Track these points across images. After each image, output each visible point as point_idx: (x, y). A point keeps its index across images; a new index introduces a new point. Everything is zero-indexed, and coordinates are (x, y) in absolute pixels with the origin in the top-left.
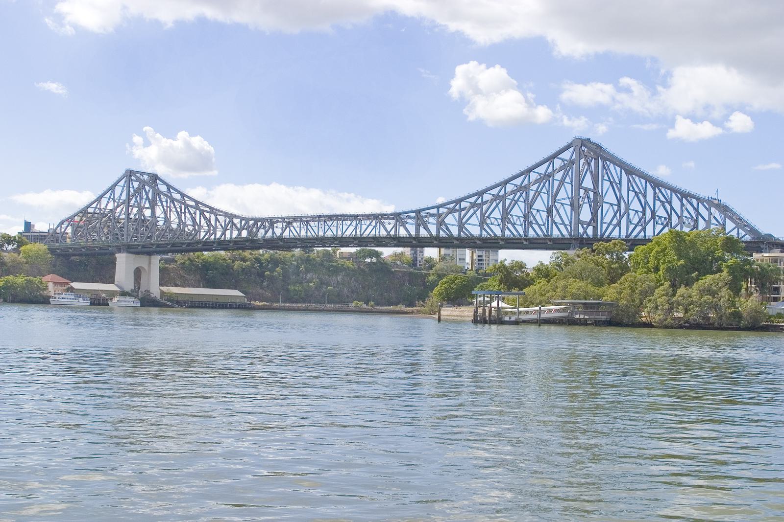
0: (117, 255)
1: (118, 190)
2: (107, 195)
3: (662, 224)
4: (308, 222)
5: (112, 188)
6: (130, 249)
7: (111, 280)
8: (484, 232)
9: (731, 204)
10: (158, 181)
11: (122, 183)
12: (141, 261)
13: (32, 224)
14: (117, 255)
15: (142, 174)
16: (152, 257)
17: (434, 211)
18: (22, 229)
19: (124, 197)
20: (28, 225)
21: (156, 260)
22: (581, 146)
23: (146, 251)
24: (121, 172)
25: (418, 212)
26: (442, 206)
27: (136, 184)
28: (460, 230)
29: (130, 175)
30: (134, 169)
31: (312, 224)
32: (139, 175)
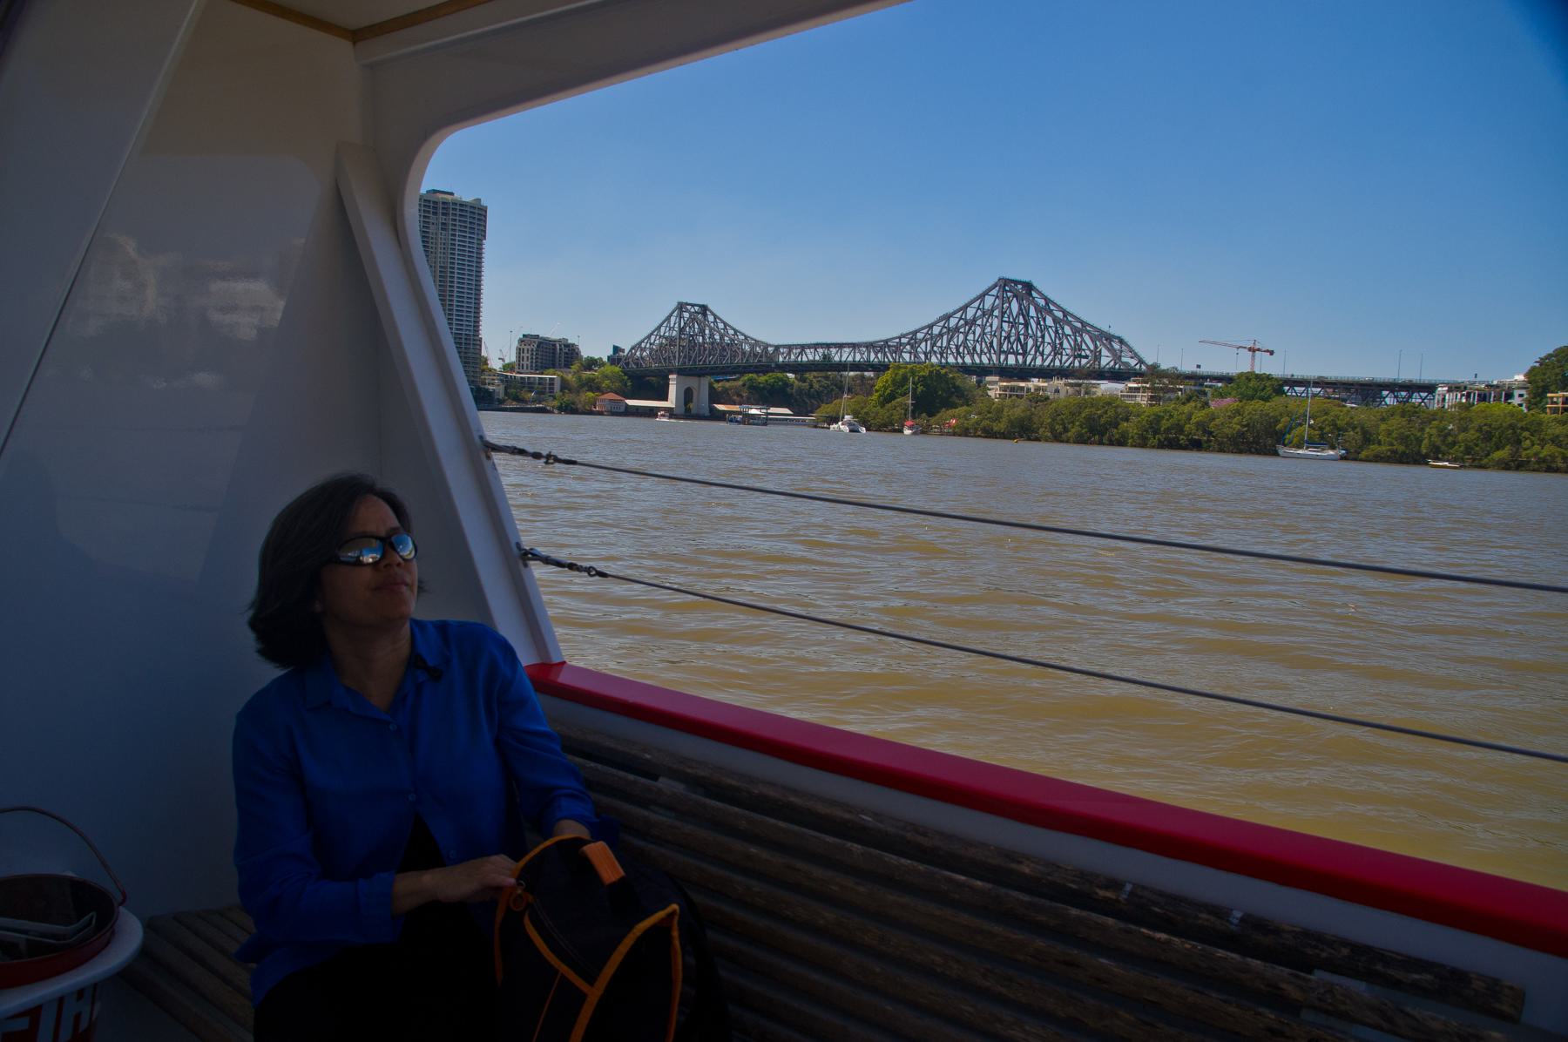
0: (670, 377)
1: (673, 319)
2: (665, 324)
3: (1067, 355)
4: (816, 350)
5: (668, 318)
6: (681, 372)
7: (666, 399)
8: (886, 360)
9: (1126, 339)
10: (708, 312)
11: (675, 314)
12: (692, 382)
13: (626, 347)
14: (670, 377)
15: (693, 305)
16: (702, 378)
17: (897, 340)
18: (611, 353)
19: (676, 325)
20: (616, 349)
21: (706, 381)
22: (1004, 286)
23: (699, 373)
24: (674, 305)
25: (886, 341)
26: (904, 336)
27: (686, 315)
28: (926, 357)
29: (681, 307)
30: (684, 300)
31: (808, 351)
32: (689, 307)
